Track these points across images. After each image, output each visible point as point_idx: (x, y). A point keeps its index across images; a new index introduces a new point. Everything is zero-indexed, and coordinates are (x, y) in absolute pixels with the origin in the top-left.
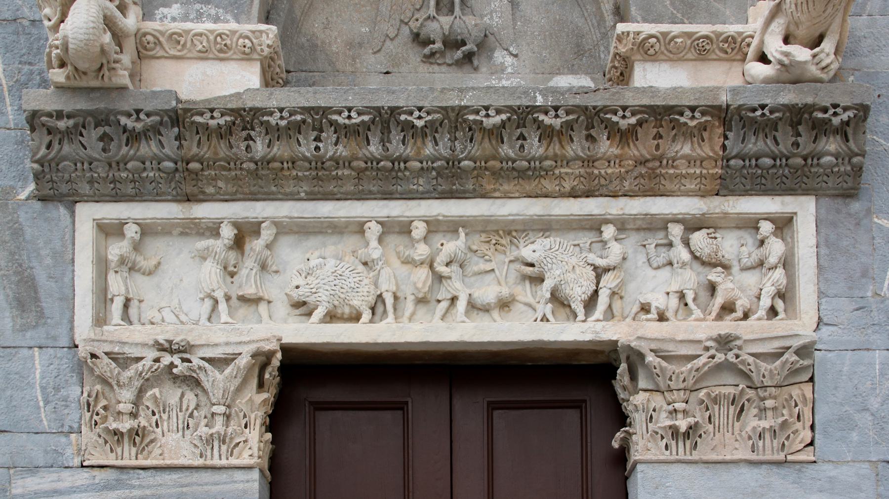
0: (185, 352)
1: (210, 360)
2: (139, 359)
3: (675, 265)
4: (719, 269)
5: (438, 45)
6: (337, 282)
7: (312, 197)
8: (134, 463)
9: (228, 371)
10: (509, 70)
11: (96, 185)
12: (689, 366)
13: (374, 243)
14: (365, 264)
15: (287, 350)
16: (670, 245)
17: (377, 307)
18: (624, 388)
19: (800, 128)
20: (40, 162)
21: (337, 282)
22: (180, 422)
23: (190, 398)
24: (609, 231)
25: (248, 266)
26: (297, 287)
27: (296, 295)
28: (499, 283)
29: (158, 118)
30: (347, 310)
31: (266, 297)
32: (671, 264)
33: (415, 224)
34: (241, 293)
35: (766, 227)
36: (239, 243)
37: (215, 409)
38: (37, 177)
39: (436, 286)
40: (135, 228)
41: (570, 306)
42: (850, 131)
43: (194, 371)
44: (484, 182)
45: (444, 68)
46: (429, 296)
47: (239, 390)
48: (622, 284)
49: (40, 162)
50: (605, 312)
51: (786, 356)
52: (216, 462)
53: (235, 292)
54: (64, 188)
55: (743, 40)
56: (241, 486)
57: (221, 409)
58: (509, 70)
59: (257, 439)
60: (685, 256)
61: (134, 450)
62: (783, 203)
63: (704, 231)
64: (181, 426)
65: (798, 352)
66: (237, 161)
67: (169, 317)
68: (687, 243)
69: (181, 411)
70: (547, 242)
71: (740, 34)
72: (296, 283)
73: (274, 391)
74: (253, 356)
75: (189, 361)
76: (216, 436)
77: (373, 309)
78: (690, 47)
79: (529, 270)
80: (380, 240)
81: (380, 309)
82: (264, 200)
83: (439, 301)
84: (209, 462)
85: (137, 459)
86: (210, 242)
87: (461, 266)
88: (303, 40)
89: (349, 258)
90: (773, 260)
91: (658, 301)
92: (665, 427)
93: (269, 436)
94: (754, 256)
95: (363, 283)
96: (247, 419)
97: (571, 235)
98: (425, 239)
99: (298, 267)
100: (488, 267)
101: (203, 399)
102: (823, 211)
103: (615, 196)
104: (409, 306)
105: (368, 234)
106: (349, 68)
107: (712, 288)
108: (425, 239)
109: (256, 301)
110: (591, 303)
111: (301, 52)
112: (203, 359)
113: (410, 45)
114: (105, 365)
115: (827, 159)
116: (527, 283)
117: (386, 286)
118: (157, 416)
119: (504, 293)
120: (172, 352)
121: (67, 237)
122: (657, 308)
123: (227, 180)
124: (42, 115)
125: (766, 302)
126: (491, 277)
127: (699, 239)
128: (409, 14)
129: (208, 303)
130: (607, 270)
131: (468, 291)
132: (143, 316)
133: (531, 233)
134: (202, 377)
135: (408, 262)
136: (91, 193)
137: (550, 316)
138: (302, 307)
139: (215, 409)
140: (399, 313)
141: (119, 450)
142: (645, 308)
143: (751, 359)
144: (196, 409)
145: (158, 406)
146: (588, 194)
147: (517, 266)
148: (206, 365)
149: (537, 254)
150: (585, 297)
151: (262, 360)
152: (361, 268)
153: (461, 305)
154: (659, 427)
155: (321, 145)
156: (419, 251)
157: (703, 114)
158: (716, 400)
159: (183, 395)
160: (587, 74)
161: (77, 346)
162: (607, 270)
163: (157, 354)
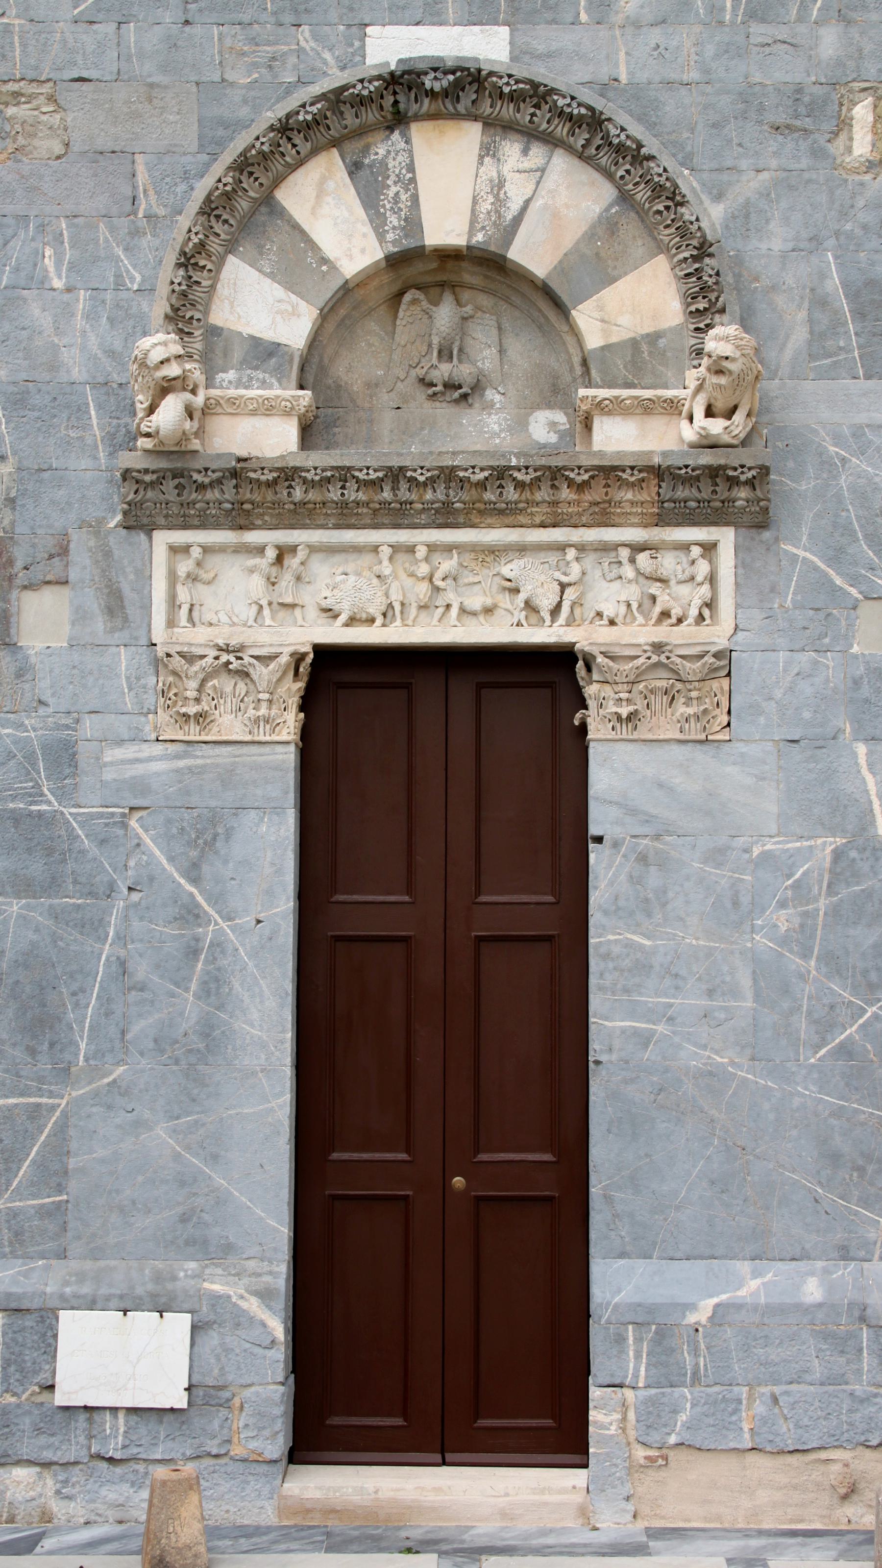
1: (257, 658)
2: (203, 657)
4: (658, 584)
5: (439, 388)
7: (337, 527)
9: (271, 666)
10: (498, 406)
12: (631, 665)
13: (386, 563)
14: (379, 577)
15: (319, 649)
18: (583, 679)
19: (718, 480)
20: (129, 504)
23: (242, 687)
24: (571, 553)
25: (286, 579)
27: (325, 604)
30: (364, 616)
32: (621, 577)
33: (418, 548)
35: (696, 551)
37: (261, 696)
38: (125, 513)
39: (435, 594)
40: (199, 550)
42: (756, 482)
45: (444, 405)
47: (279, 680)
48: (581, 597)
49: (129, 504)
50: (568, 619)
51: (706, 658)
52: (262, 738)
53: (276, 600)
54: (145, 521)
56: (280, 757)
57: (266, 696)
58: (498, 406)
59: (293, 720)
62: (708, 532)
63: (648, 552)
65: (715, 656)
66: (279, 504)
67: (224, 619)
68: (632, 561)
70: (522, 562)
71: (676, 397)
73: (306, 679)
74: (291, 655)
75: (241, 658)
77: (384, 615)
80: (391, 559)
81: (390, 614)
84: (256, 739)
86: (257, 561)
87: (455, 579)
88: (330, 381)
89: (366, 573)
90: (699, 579)
91: (609, 611)
93: (302, 715)
94: (687, 572)
97: (542, 554)
98: (427, 559)
101: (251, 687)
102: (740, 539)
103: (575, 526)
104: (413, 611)
105: (381, 555)
106: (367, 405)
107: (654, 599)
108: (427, 559)
109: (293, 606)
110: (555, 611)
111: (329, 392)
112: (252, 656)
113: (417, 385)
114: (177, 662)
115: (739, 503)
116: (507, 593)
117: (396, 597)
120: (228, 651)
121: (146, 558)
123: (272, 516)
125: (694, 612)
126: (476, 588)
127: (643, 558)
128: (416, 360)
129: (255, 608)
130: (570, 585)
131: (460, 600)
133: (510, 553)
134: (251, 671)
135: (412, 575)
137: (524, 622)
138: (330, 613)
139: (261, 696)
140: (405, 616)
142: (599, 615)
143: (679, 660)
147: (497, 579)
149: (513, 573)
150: (551, 607)
151: (298, 659)
152: (375, 581)
153: (454, 611)
155: (345, 492)
156: (421, 570)
159: (236, 684)
160: (561, 408)
162: (570, 585)
163: (216, 653)
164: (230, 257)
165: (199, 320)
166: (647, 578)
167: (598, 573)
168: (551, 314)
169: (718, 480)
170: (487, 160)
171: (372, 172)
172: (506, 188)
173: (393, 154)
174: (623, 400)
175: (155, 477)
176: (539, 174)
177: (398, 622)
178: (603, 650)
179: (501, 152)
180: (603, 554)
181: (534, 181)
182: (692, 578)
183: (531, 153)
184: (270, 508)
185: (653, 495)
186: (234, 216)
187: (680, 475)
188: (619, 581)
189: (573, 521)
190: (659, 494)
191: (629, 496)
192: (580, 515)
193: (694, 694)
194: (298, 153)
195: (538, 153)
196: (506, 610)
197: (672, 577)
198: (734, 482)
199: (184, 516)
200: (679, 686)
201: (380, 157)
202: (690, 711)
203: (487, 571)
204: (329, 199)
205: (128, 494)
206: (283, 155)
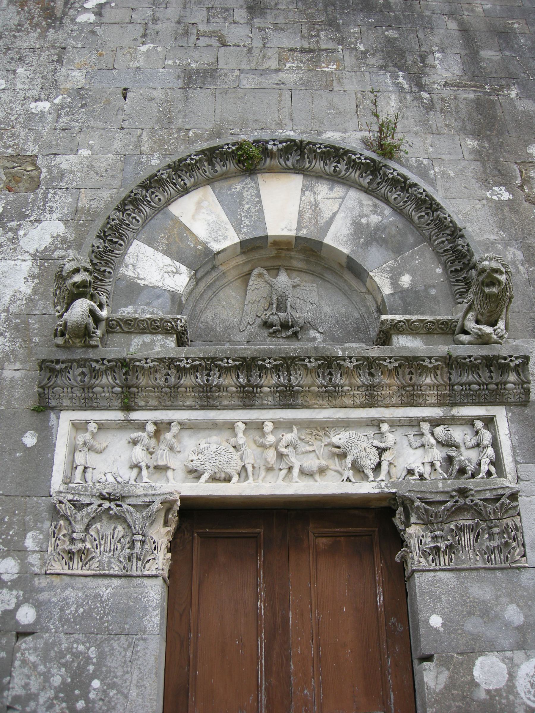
0: (118, 500)
1: (134, 506)
3: (427, 447)
6: (217, 458)
8: (80, 572)
11: (74, 401)
13: (240, 435)
15: (183, 499)
16: (422, 435)
17: (243, 472)
21: (217, 458)
22: (112, 546)
24: (385, 427)
26: (192, 461)
27: (190, 466)
28: (318, 458)
29: (115, 363)
30: (223, 475)
31: (172, 467)
32: (423, 446)
33: (266, 423)
34: (155, 464)
35: (479, 424)
36: (157, 434)
41: (363, 472)
43: (124, 512)
44: (308, 399)
46: (274, 466)
55: (452, 324)
60: (433, 441)
61: (80, 564)
62: (486, 410)
64: (112, 548)
68: (432, 434)
69: (113, 538)
70: (347, 434)
71: (450, 320)
72: (191, 459)
73: (174, 526)
75: (120, 506)
76: (135, 555)
79: (337, 450)
80: (244, 432)
81: (243, 475)
82: (174, 409)
83: (281, 470)
85: (82, 569)
92: (430, 548)
93: (169, 555)
95: (233, 458)
96: (156, 544)
97: (362, 429)
99: (192, 449)
100: (311, 449)
103: (387, 407)
118: (97, 542)
119: (322, 464)
120: (110, 500)
122: (418, 472)
124: (48, 362)
126: (312, 455)
127: (439, 430)
132: (94, 478)
136: (71, 405)
141: (71, 563)
144: (123, 537)
145: (99, 534)
146: (371, 406)
148: (131, 509)
149: (341, 441)
152: (232, 449)
154: (427, 548)
156: (269, 439)
157: (436, 360)
158: (460, 529)
159: (115, 528)
161: (51, 496)
164: (136, 241)
165: (110, 273)
166: (443, 445)
167: (406, 442)
168: (354, 283)
169: (492, 368)
171: (233, 198)
173: (246, 189)
174: (414, 322)
175: (63, 366)
177: (251, 479)
178: (419, 496)
180: (409, 429)
182: (478, 445)
183: (335, 190)
184: (151, 391)
185: (446, 380)
186: (140, 216)
187: (465, 364)
188: (422, 449)
189: (385, 402)
190: (450, 379)
191: (428, 381)
192: (391, 396)
193: (496, 530)
194: (185, 184)
195: (339, 191)
196: (336, 471)
197: (462, 445)
198: (504, 369)
199: (85, 398)
200: (483, 525)
201: (238, 190)
202: (496, 543)
203: (319, 443)
204: (204, 211)
205: (43, 380)
206: (175, 184)
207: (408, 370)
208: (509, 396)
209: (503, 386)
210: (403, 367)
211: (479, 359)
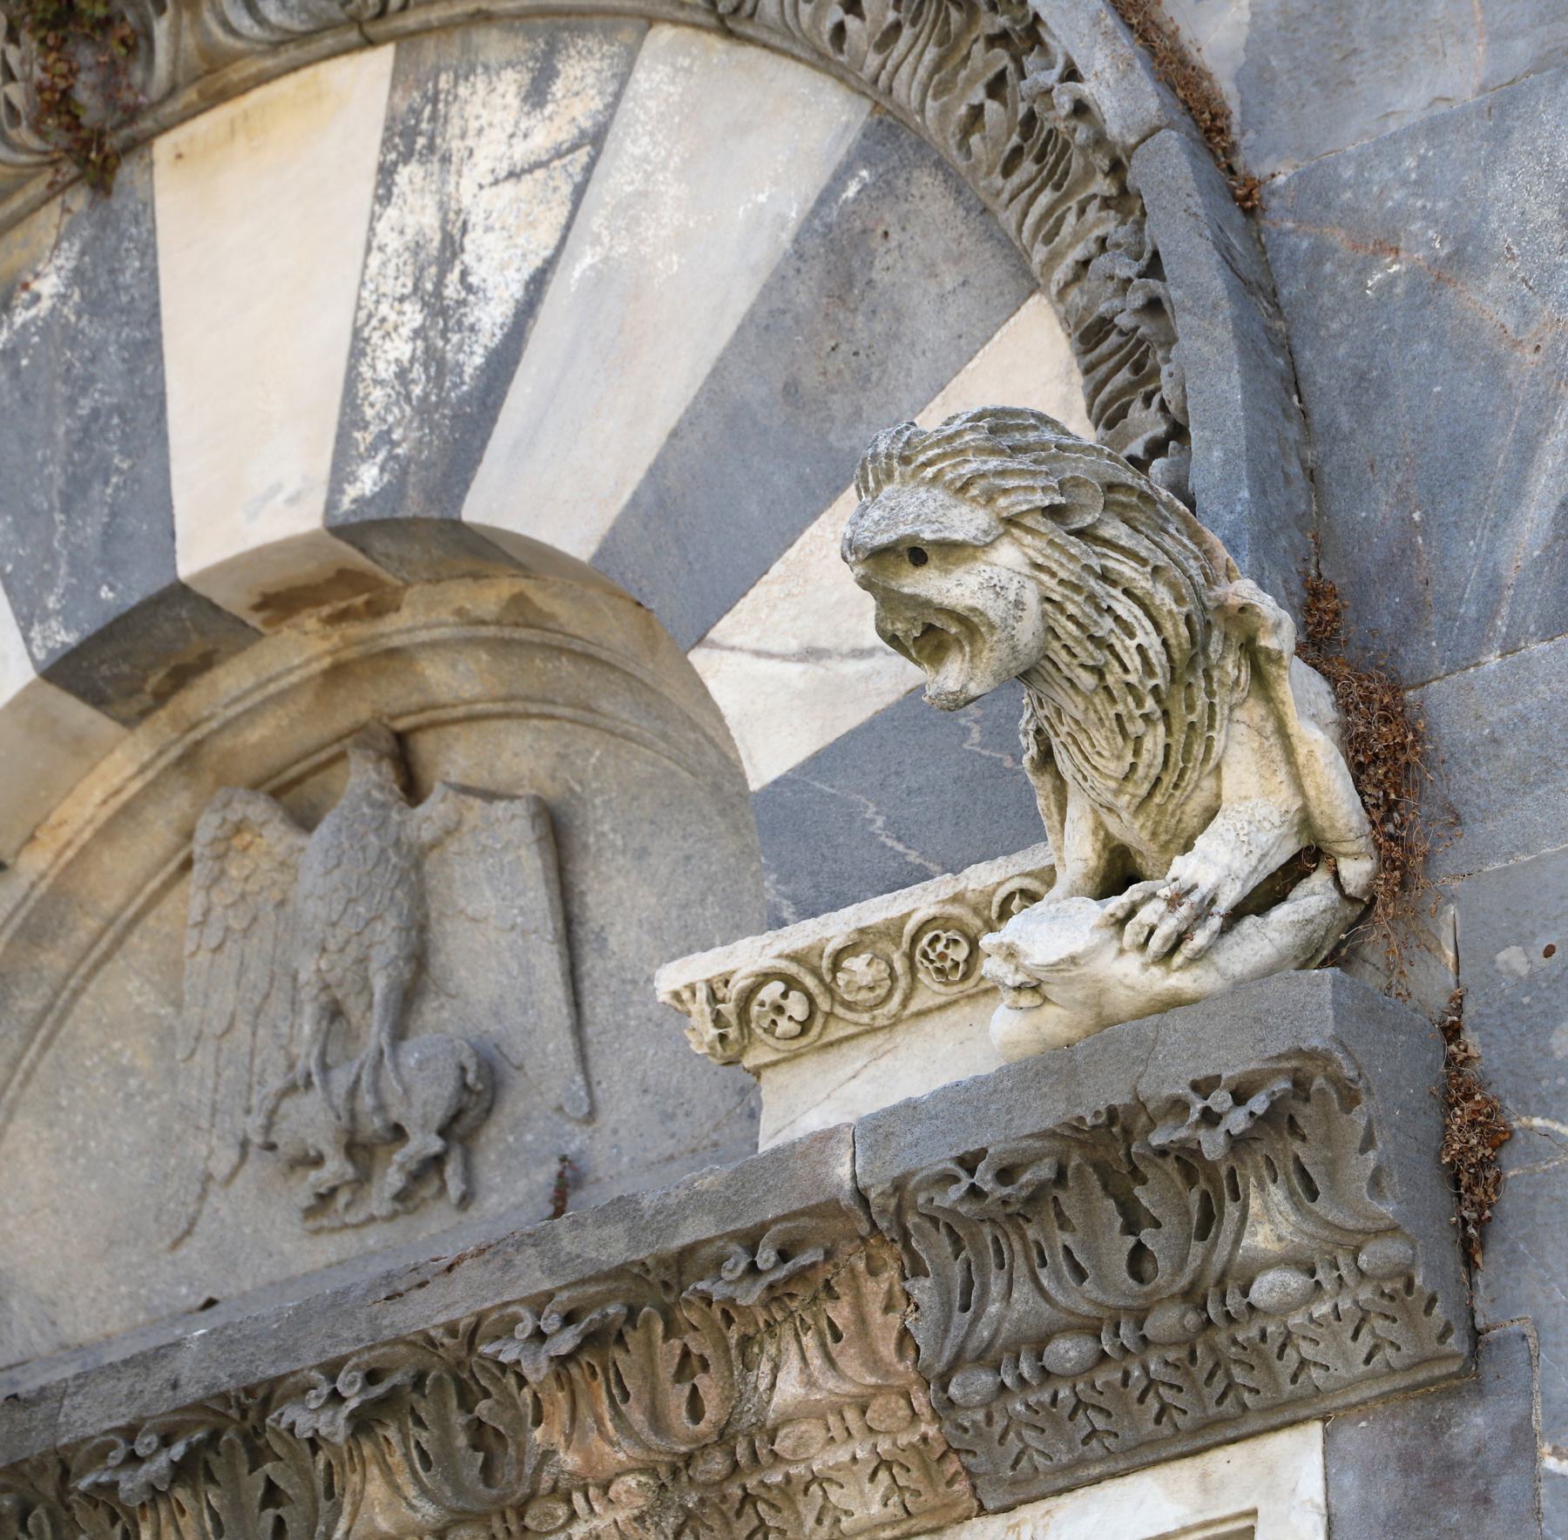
78: (912, 969)
170: (406, 175)
172: (468, 258)
176: (582, 156)
179: (454, 128)
181: (567, 190)
207: (668, 1354)
208: (1307, 1350)
209: (1234, 1302)
210: (633, 1338)
211: (1038, 1158)
